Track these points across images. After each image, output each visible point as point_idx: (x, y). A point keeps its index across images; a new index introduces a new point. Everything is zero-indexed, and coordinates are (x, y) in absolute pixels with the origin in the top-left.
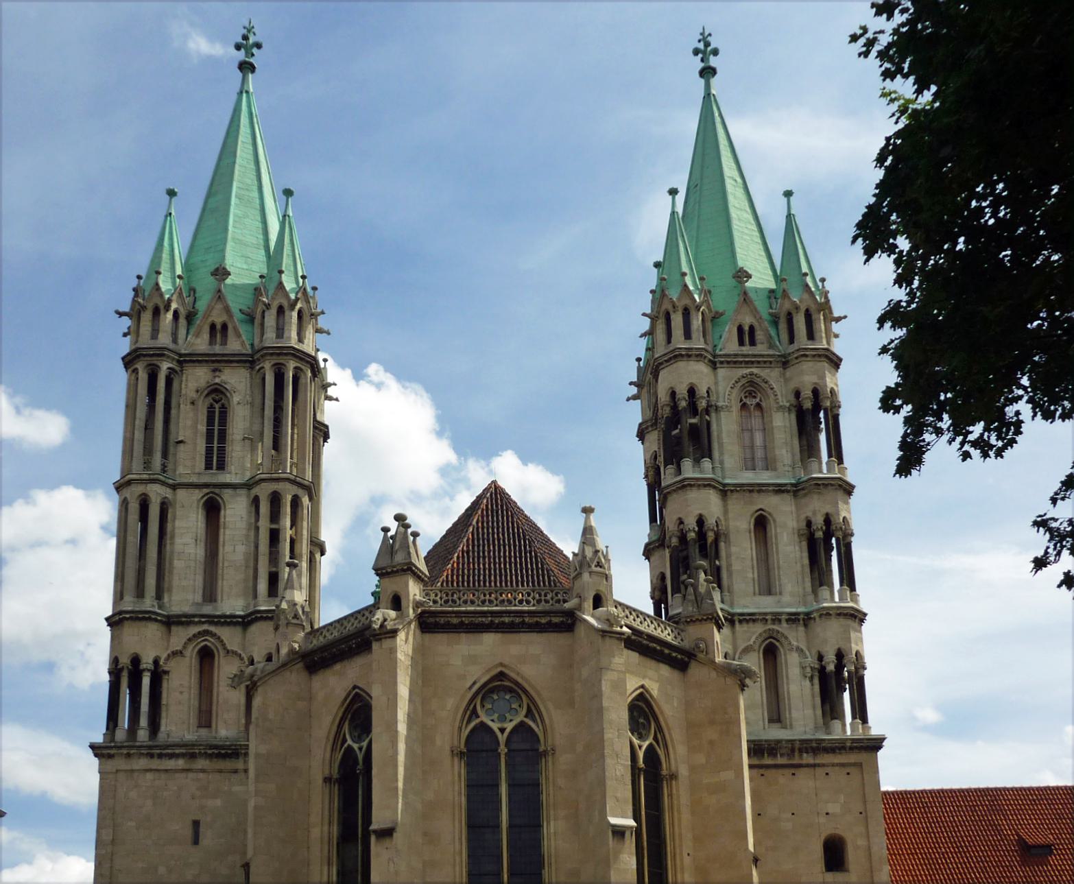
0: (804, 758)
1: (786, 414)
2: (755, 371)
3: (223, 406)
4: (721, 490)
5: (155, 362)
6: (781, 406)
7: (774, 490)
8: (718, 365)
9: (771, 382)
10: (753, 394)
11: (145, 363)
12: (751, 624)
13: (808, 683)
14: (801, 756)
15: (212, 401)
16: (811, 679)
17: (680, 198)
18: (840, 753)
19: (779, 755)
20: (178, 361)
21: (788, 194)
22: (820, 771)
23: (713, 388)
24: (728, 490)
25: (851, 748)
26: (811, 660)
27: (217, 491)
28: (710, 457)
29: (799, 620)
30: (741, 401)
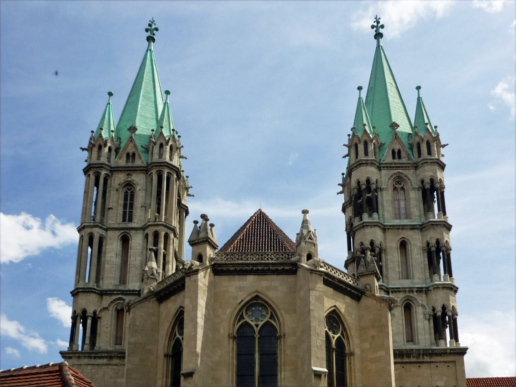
0: (425, 359)
1: (417, 192)
2: (401, 171)
3: (132, 192)
4: (383, 228)
5: (98, 171)
6: (414, 188)
7: (410, 228)
8: (382, 169)
9: (409, 176)
10: (400, 183)
11: (94, 171)
12: (398, 293)
13: (427, 322)
14: (423, 357)
15: (127, 190)
16: (429, 320)
18: (444, 356)
19: (412, 357)
20: (111, 171)
22: (433, 365)
23: (379, 180)
24: (386, 228)
25: (450, 354)
26: (429, 310)
27: (128, 231)
28: (377, 212)
29: (423, 291)
30: (393, 186)
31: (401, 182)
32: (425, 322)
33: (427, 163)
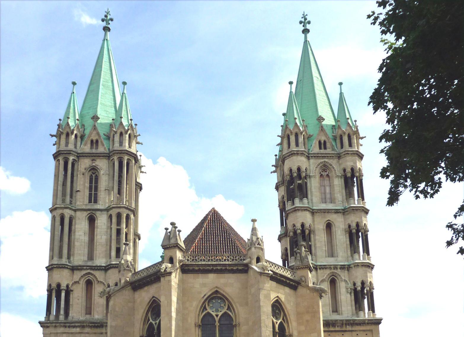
0: (348, 328)
1: (340, 179)
2: (326, 160)
3: (96, 176)
4: (311, 212)
5: (67, 157)
6: (338, 176)
8: (310, 158)
9: (333, 165)
10: (326, 170)
11: (63, 157)
12: (324, 270)
13: (349, 295)
14: (346, 327)
15: (91, 173)
16: (351, 293)
17: (294, 86)
18: (363, 326)
19: (336, 326)
20: (77, 156)
21: (341, 84)
22: (354, 333)
23: (308, 168)
24: (315, 212)
25: (368, 323)
26: (350, 285)
27: (94, 212)
28: (307, 198)
29: (345, 268)
30: (320, 173)
31: (326, 170)
32: (347, 295)
33: (348, 154)
